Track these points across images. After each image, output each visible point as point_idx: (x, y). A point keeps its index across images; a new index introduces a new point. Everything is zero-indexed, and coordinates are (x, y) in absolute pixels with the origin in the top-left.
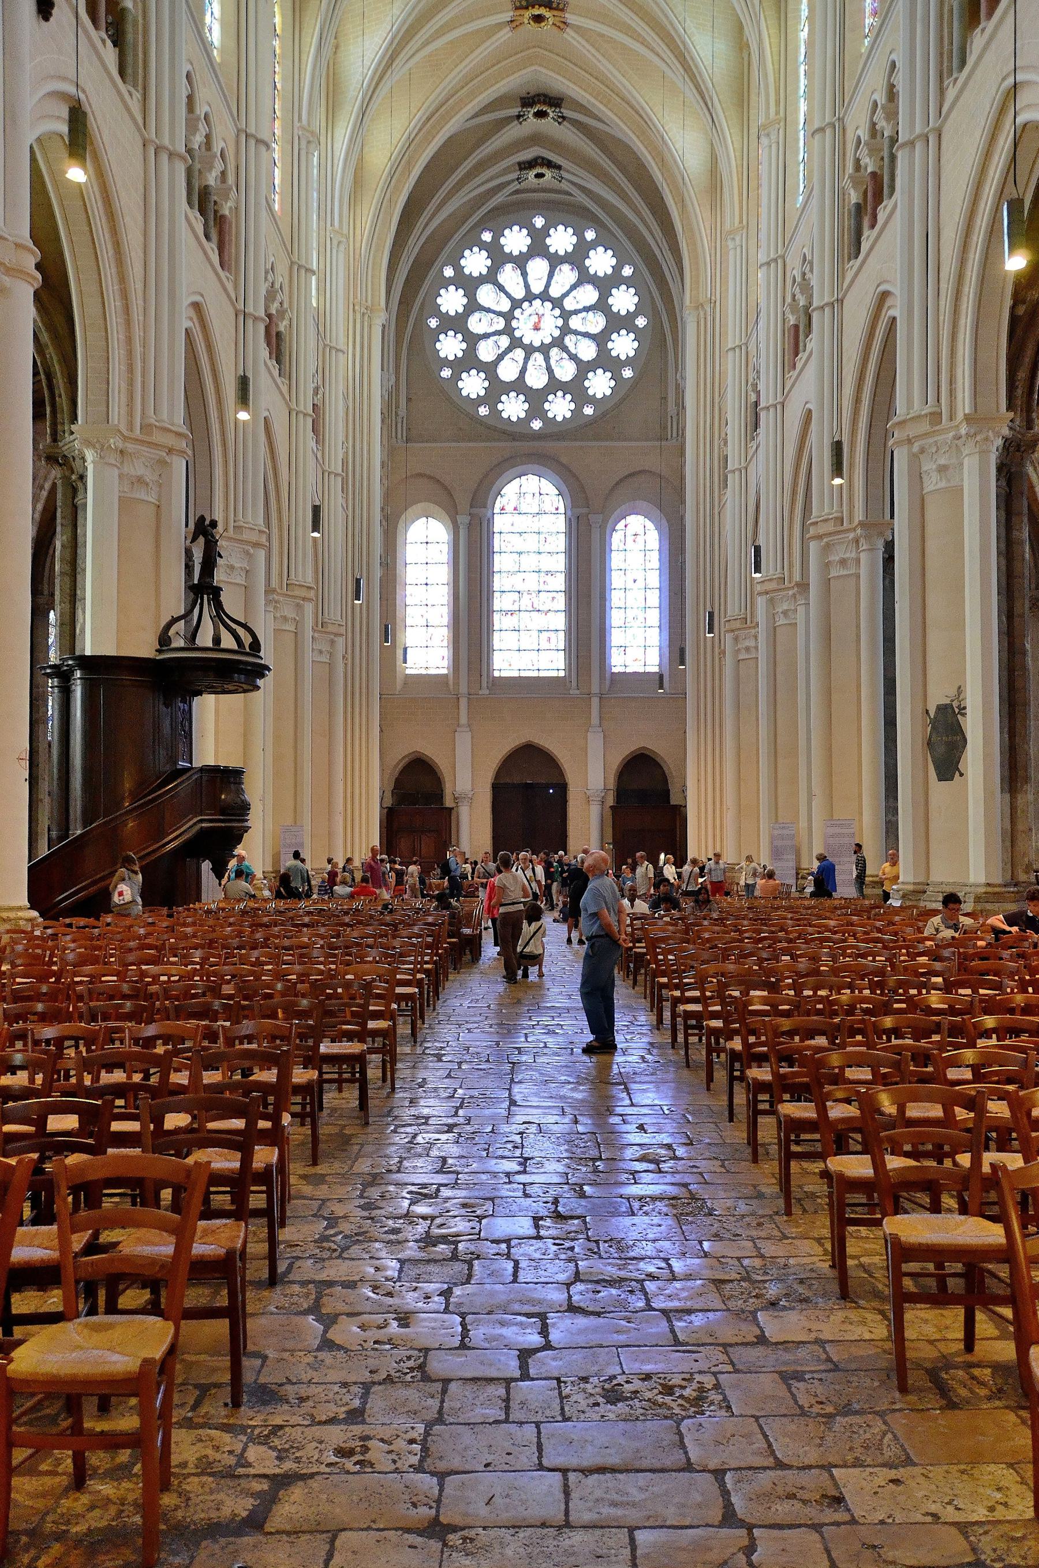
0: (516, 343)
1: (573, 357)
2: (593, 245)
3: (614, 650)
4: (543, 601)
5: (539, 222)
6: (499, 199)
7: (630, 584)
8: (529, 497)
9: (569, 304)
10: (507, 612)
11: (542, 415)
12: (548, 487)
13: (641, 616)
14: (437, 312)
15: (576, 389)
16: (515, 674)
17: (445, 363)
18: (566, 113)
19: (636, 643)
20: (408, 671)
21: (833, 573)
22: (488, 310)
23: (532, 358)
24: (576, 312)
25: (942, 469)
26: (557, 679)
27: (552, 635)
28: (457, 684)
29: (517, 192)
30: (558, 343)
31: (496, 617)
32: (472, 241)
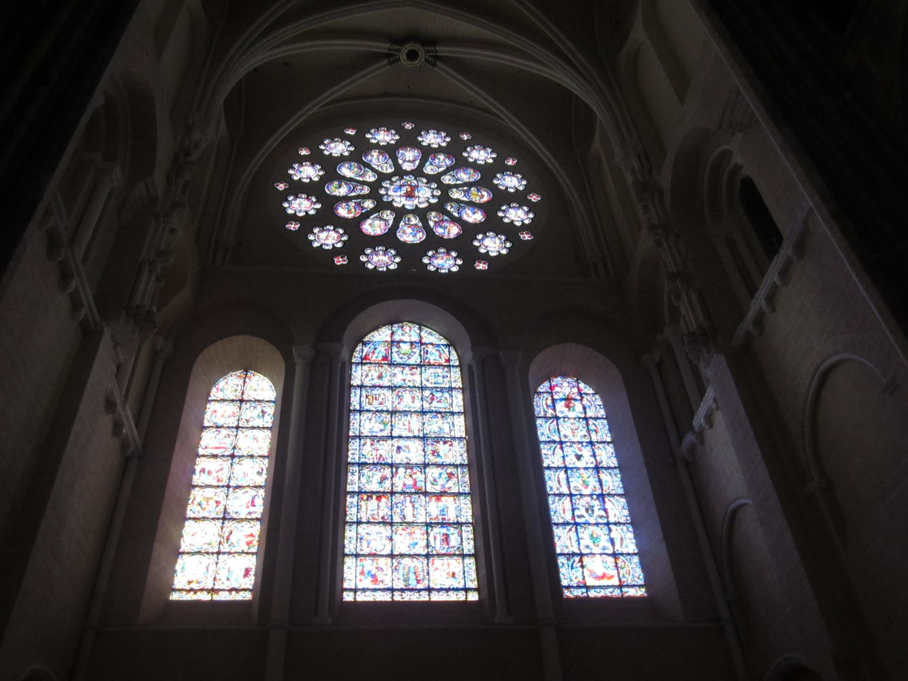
0: (382, 205)
3: (561, 560)
4: (435, 479)
5: (408, 126)
7: (571, 461)
8: (405, 348)
9: (447, 180)
12: (430, 337)
13: (596, 504)
15: (463, 245)
17: (294, 218)
20: (175, 596)
24: (456, 186)
26: (466, 603)
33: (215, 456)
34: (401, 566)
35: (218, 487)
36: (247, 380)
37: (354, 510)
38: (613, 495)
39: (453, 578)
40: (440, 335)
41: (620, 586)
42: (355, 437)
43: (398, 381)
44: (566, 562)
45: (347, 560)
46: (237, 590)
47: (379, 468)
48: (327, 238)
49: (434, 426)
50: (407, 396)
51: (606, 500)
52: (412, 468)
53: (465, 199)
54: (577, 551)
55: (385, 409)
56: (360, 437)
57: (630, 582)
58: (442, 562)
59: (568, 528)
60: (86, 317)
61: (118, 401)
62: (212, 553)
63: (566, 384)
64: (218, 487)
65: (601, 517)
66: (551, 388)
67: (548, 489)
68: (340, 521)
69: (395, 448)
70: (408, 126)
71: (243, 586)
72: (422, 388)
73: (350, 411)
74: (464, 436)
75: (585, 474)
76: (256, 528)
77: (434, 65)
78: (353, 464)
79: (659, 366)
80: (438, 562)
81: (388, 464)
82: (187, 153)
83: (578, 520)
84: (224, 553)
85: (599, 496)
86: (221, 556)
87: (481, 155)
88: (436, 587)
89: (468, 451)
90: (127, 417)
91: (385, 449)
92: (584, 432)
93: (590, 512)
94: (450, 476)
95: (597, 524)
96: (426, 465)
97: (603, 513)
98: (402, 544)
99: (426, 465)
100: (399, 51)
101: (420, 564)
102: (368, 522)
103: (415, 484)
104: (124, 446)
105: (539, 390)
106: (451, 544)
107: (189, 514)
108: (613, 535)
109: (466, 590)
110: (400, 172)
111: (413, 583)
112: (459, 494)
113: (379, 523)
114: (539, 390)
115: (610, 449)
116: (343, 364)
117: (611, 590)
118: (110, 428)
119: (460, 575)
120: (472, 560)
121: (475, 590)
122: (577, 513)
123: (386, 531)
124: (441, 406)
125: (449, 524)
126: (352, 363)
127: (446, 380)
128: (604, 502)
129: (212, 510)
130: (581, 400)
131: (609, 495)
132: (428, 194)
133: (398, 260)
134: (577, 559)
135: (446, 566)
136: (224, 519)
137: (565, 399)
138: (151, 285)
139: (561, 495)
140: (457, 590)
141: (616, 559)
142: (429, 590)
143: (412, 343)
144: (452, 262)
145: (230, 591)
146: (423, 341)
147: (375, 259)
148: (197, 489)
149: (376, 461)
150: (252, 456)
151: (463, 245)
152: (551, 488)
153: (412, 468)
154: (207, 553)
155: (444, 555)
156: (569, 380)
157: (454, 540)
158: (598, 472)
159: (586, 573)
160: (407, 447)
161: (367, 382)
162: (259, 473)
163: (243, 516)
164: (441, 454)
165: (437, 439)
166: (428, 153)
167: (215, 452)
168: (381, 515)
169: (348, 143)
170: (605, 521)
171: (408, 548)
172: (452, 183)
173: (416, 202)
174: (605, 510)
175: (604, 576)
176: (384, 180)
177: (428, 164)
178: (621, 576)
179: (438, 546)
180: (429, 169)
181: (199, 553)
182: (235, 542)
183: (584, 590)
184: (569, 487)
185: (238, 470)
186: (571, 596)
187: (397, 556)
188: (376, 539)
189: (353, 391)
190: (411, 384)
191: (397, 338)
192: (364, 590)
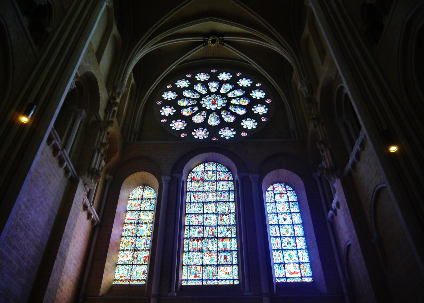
0: (202, 109)
4: (222, 231)
5: (214, 71)
7: (281, 221)
8: (210, 173)
9: (230, 95)
10: (194, 239)
13: (292, 240)
15: (236, 126)
17: (164, 117)
19: (292, 261)
22: (189, 98)
24: (234, 98)
26: (233, 285)
27: (228, 254)
30: (226, 108)
33: (131, 223)
34: (207, 270)
35: (132, 236)
36: (144, 190)
37: (187, 246)
38: (299, 237)
39: (228, 275)
40: (225, 167)
41: (301, 277)
42: (188, 214)
43: (206, 188)
44: (278, 267)
45: (184, 267)
46: (140, 280)
47: (198, 227)
48: (178, 125)
49: (222, 208)
50: (210, 195)
51: (296, 238)
52: (212, 227)
53: (238, 104)
54: (283, 262)
55: (201, 201)
56: (190, 214)
57: (306, 275)
58: (223, 268)
59: (279, 251)
60: (72, 175)
61: (89, 205)
62: (130, 265)
63: (280, 187)
64: (132, 236)
65: (294, 246)
66: (274, 189)
67: (271, 234)
68: (181, 251)
69: (205, 218)
70: (214, 71)
71: (142, 279)
72: (217, 191)
73: (186, 202)
74: (234, 212)
75: (288, 227)
76: (147, 254)
77: (224, 45)
78: (187, 226)
79: (320, 178)
80: (222, 268)
81: (202, 225)
82: (114, 99)
83: (283, 248)
84: (135, 264)
85: (293, 237)
86: (133, 266)
87: (245, 83)
88: (221, 279)
89: (236, 219)
90: (93, 211)
91: (200, 218)
92: (288, 208)
93: (289, 244)
94: (228, 230)
95: (292, 250)
96: (217, 226)
97: (295, 245)
98: (207, 260)
99: (217, 226)
100: (208, 40)
101: (214, 269)
102: (193, 251)
103: (213, 235)
104: (93, 222)
105: (268, 190)
106: (228, 260)
108: (299, 254)
109: (234, 280)
110: (209, 93)
111: (211, 277)
112: (232, 238)
113: (198, 251)
114: (268, 190)
115: (298, 215)
116: (183, 182)
117: (297, 279)
118: (86, 216)
119: (231, 274)
120: (237, 267)
121: (237, 280)
122: (283, 245)
123: (200, 255)
124: (225, 199)
125: (227, 251)
126: (187, 181)
127: (227, 187)
128: (296, 239)
129: (130, 247)
130: (287, 193)
131: (298, 236)
132: (222, 103)
133: (208, 133)
134: (282, 265)
135: (225, 269)
136: (135, 250)
137: (280, 194)
138: (99, 158)
139: (276, 237)
140: (230, 279)
141: (300, 265)
142: (218, 280)
143: (213, 171)
144: (231, 133)
145: (137, 280)
146: (218, 170)
147: (199, 133)
148: (124, 237)
149: (197, 224)
150: (146, 223)
151: (236, 126)
152: (272, 234)
153: (212, 227)
154: (128, 265)
155: (224, 265)
156: (282, 184)
157: (229, 258)
158: (293, 226)
159: (286, 271)
160: (210, 218)
161: (194, 189)
162: (148, 230)
163: (142, 249)
164: (225, 220)
165: (223, 214)
166: (221, 83)
167: (131, 221)
168: (198, 248)
169: (188, 81)
170: (296, 248)
172: (233, 96)
173: (216, 106)
174: (296, 243)
175: (294, 273)
176: (203, 97)
177: (222, 88)
178: (302, 272)
179: (222, 261)
180: (222, 91)
181: (125, 264)
182: (139, 259)
183: (285, 279)
184: (280, 233)
185: (140, 229)
186: (280, 282)
187: (205, 265)
188: (196, 258)
189: (187, 193)
190: (212, 190)
191: (207, 169)
192: (191, 280)
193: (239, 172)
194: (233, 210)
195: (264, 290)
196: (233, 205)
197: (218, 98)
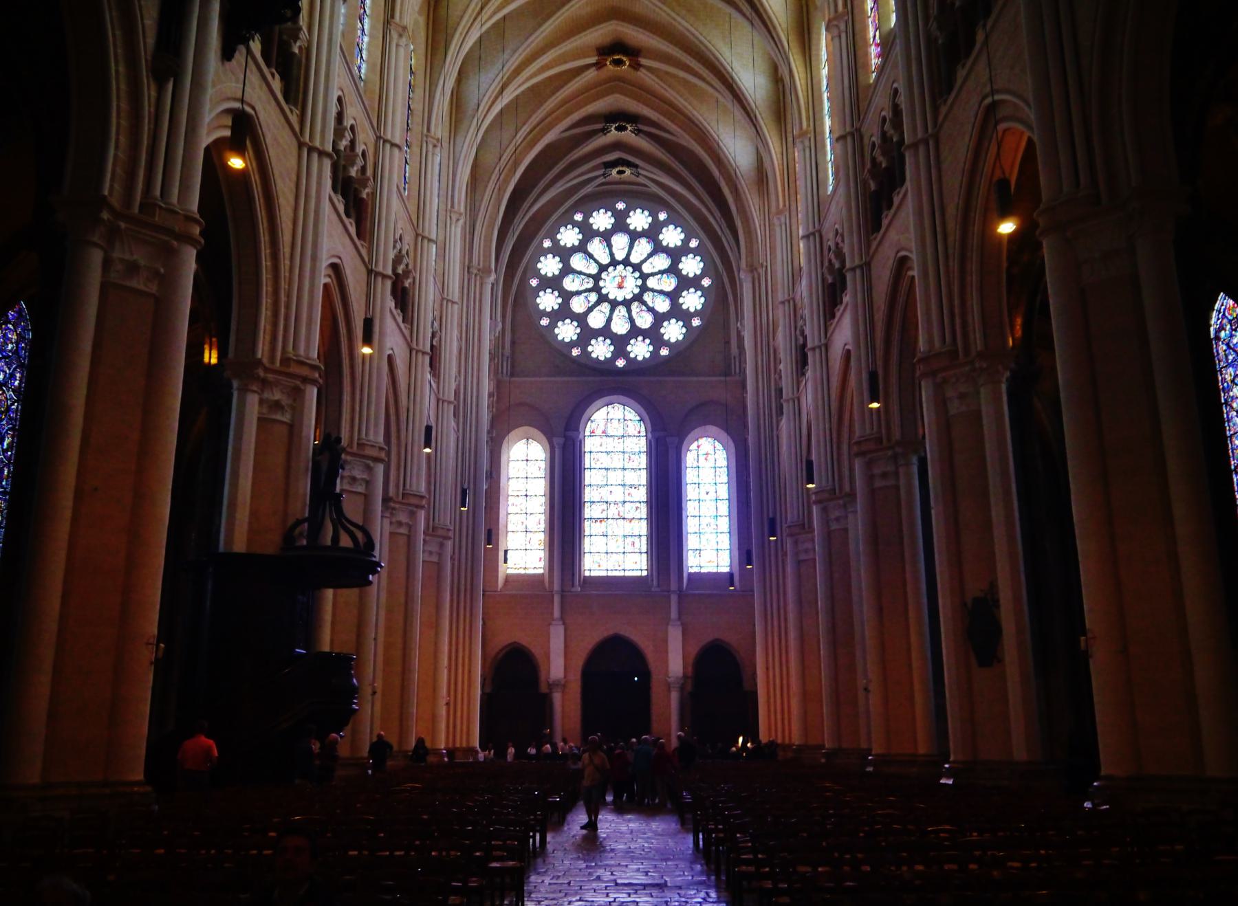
0: (603, 298)
1: (651, 310)
2: (665, 224)
3: (690, 553)
4: (629, 512)
5: (621, 206)
6: (589, 189)
8: (615, 423)
9: (646, 268)
11: (626, 355)
12: (631, 414)
13: (713, 521)
14: (537, 273)
15: (653, 334)
16: (604, 574)
17: (544, 314)
18: (641, 127)
19: (710, 547)
20: (509, 571)
21: (878, 483)
22: (580, 273)
23: (617, 311)
24: (653, 274)
25: (962, 396)
27: (636, 540)
28: (551, 582)
29: (602, 184)
30: (638, 298)
31: (587, 524)
32: (567, 220)
39: (635, 564)
48: (567, 331)
50: (616, 457)
70: (621, 206)
76: (542, 536)
107: (510, 529)
171: (615, 547)
180: (635, 259)
193: (653, 431)
194: (644, 481)
195: (674, 586)
196: (644, 474)
197: (629, 274)
